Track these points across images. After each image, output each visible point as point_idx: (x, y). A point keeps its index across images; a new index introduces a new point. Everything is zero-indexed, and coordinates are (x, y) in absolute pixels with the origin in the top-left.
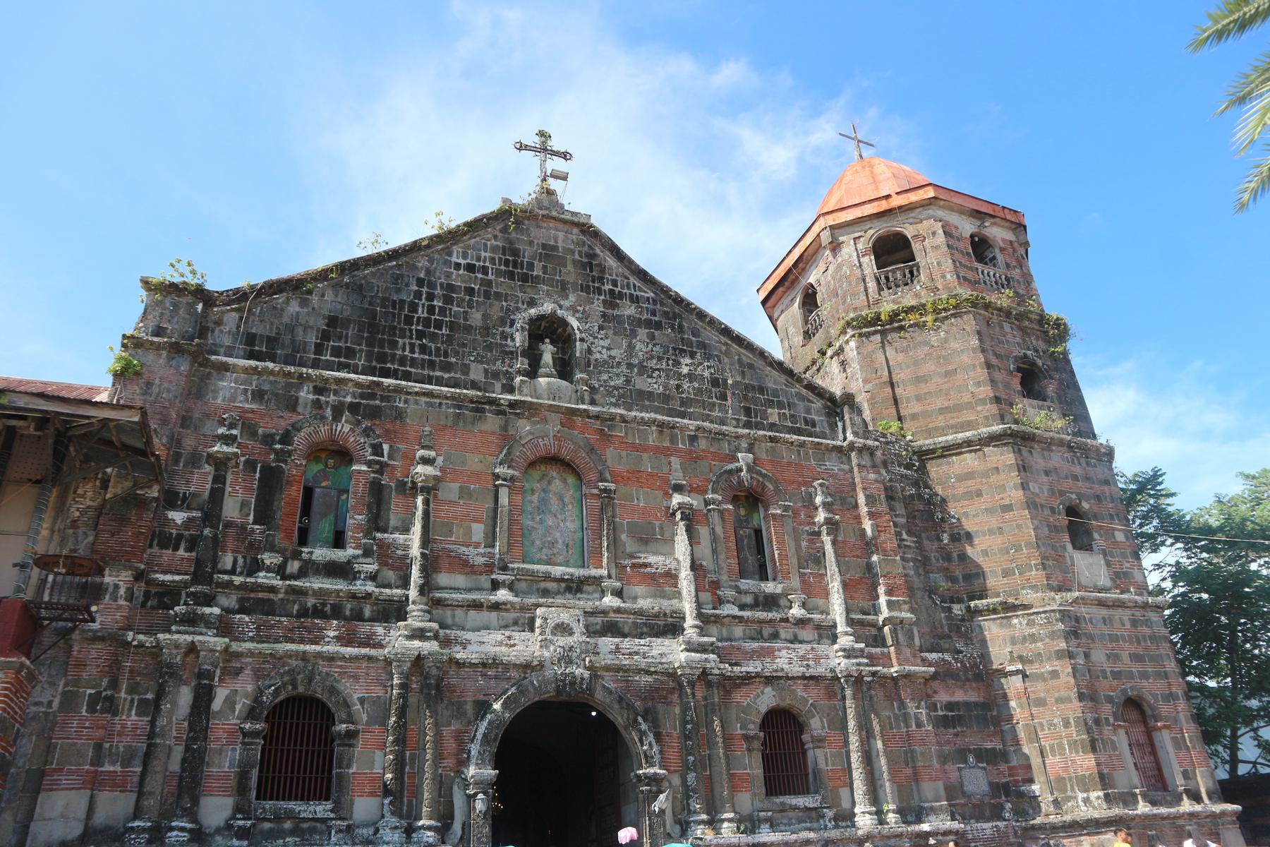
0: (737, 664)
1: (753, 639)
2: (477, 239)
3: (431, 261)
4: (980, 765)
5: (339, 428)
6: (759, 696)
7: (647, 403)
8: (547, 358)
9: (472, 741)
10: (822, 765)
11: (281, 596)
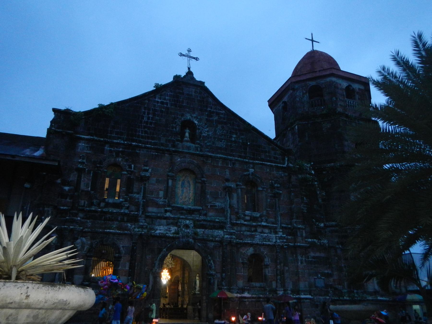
0: (241, 239)
1: (248, 231)
2: (165, 92)
3: (149, 100)
4: (322, 278)
5: (118, 160)
6: (248, 250)
7: (219, 151)
8: (187, 134)
9: (156, 260)
10: (267, 273)
11: (99, 214)
